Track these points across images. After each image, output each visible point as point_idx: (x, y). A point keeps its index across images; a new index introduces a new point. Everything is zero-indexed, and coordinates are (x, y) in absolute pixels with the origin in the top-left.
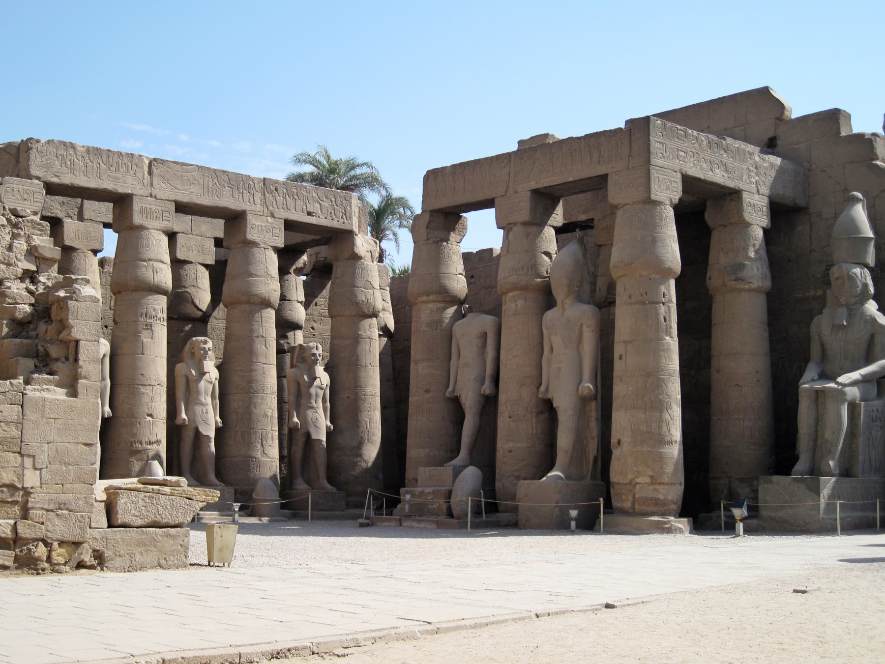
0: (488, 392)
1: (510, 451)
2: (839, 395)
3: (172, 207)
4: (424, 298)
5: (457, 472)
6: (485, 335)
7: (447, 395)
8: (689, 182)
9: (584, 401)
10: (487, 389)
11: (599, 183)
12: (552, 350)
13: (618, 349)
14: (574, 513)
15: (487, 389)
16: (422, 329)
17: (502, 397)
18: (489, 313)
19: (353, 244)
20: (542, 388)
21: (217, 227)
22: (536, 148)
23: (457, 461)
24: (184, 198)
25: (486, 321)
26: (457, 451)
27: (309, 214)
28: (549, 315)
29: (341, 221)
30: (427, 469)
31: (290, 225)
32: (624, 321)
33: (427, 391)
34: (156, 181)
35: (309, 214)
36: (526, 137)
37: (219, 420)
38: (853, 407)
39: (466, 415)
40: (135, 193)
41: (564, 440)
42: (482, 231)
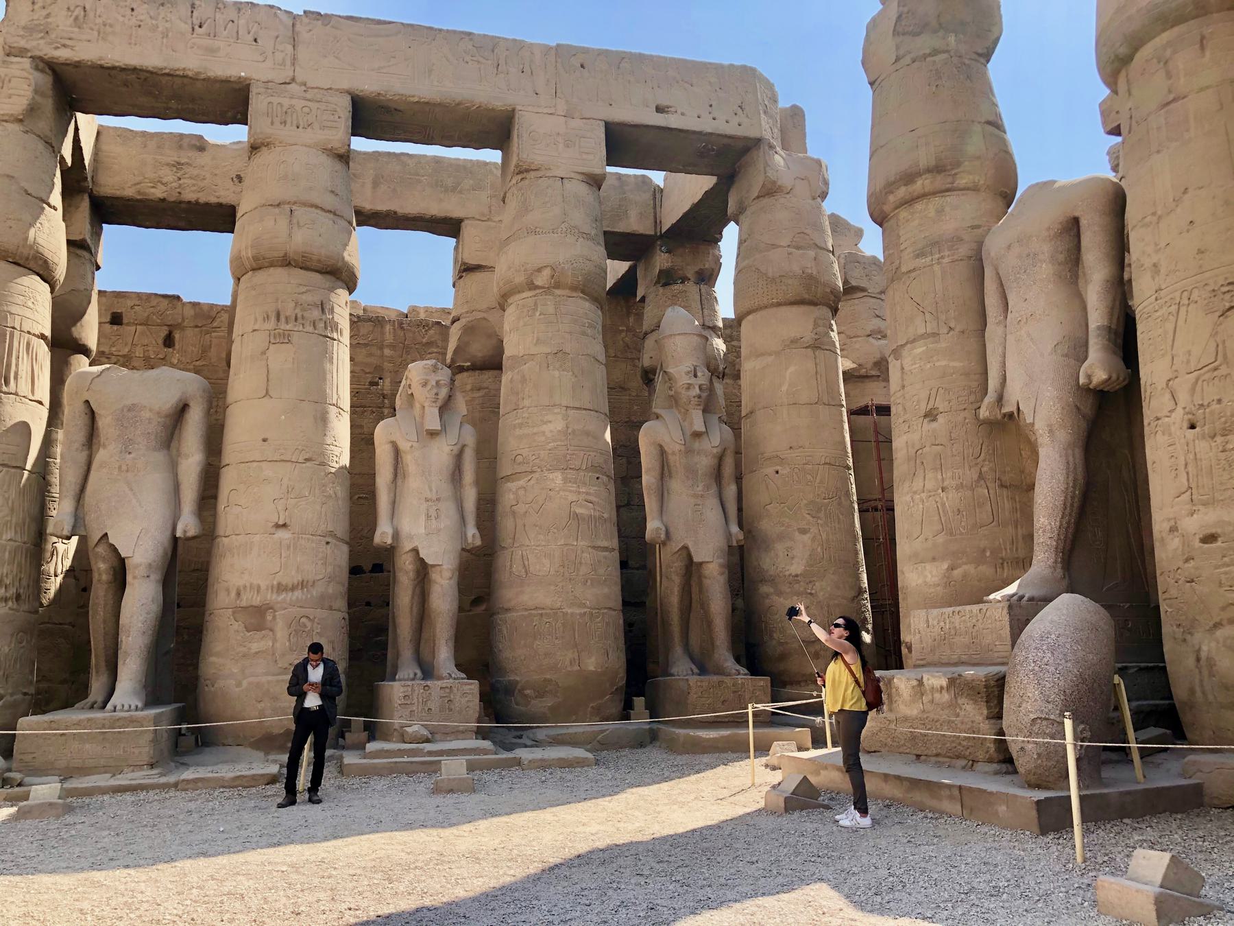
0: (1100, 376)
1: (1210, 538)
3: (346, 102)
4: (902, 192)
5: (1021, 614)
6: (1073, 227)
7: (984, 413)
10: (1098, 367)
15: (1098, 367)
16: (904, 269)
17: (1152, 370)
19: (766, 165)
24: (369, 85)
26: (1024, 563)
27: (659, 109)
29: (736, 120)
30: (935, 612)
33: (931, 415)
34: (302, 53)
37: (472, 531)
39: (1042, 452)
40: (254, 76)
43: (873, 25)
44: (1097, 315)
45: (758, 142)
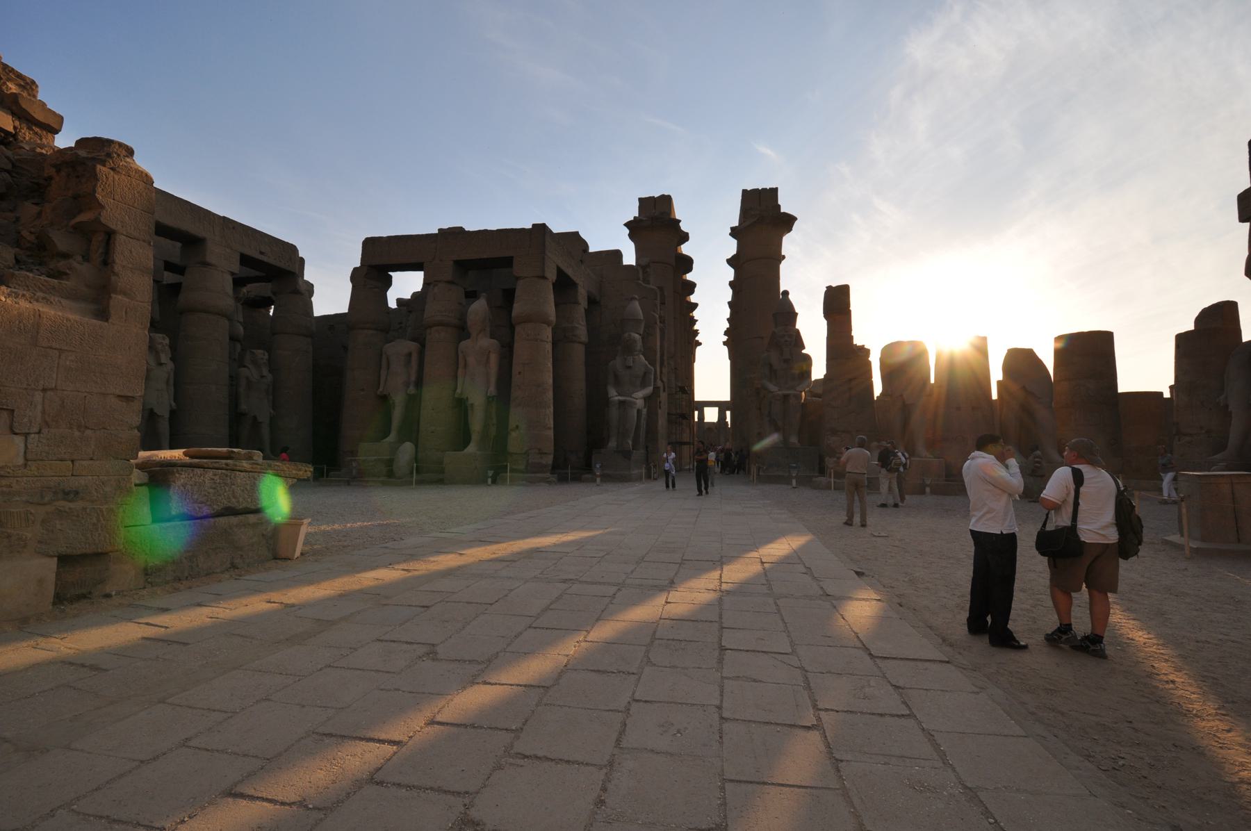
2: (631, 404)
6: (410, 355)
8: (560, 272)
9: (489, 400)
11: (508, 262)
12: (465, 365)
13: (516, 369)
14: (490, 473)
18: (413, 340)
20: (459, 391)
21: (173, 249)
22: (454, 234)
23: (392, 437)
25: (413, 346)
26: (386, 433)
27: (262, 253)
28: (463, 344)
31: (245, 260)
32: (521, 350)
35: (262, 253)
36: (446, 227)
38: (639, 411)
41: (476, 424)
42: (406, 284)
43: (355, 269)
44: (413, 378)
45: (293, 274)
